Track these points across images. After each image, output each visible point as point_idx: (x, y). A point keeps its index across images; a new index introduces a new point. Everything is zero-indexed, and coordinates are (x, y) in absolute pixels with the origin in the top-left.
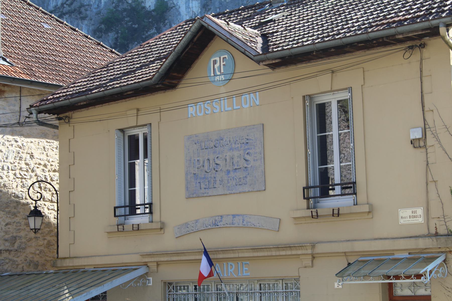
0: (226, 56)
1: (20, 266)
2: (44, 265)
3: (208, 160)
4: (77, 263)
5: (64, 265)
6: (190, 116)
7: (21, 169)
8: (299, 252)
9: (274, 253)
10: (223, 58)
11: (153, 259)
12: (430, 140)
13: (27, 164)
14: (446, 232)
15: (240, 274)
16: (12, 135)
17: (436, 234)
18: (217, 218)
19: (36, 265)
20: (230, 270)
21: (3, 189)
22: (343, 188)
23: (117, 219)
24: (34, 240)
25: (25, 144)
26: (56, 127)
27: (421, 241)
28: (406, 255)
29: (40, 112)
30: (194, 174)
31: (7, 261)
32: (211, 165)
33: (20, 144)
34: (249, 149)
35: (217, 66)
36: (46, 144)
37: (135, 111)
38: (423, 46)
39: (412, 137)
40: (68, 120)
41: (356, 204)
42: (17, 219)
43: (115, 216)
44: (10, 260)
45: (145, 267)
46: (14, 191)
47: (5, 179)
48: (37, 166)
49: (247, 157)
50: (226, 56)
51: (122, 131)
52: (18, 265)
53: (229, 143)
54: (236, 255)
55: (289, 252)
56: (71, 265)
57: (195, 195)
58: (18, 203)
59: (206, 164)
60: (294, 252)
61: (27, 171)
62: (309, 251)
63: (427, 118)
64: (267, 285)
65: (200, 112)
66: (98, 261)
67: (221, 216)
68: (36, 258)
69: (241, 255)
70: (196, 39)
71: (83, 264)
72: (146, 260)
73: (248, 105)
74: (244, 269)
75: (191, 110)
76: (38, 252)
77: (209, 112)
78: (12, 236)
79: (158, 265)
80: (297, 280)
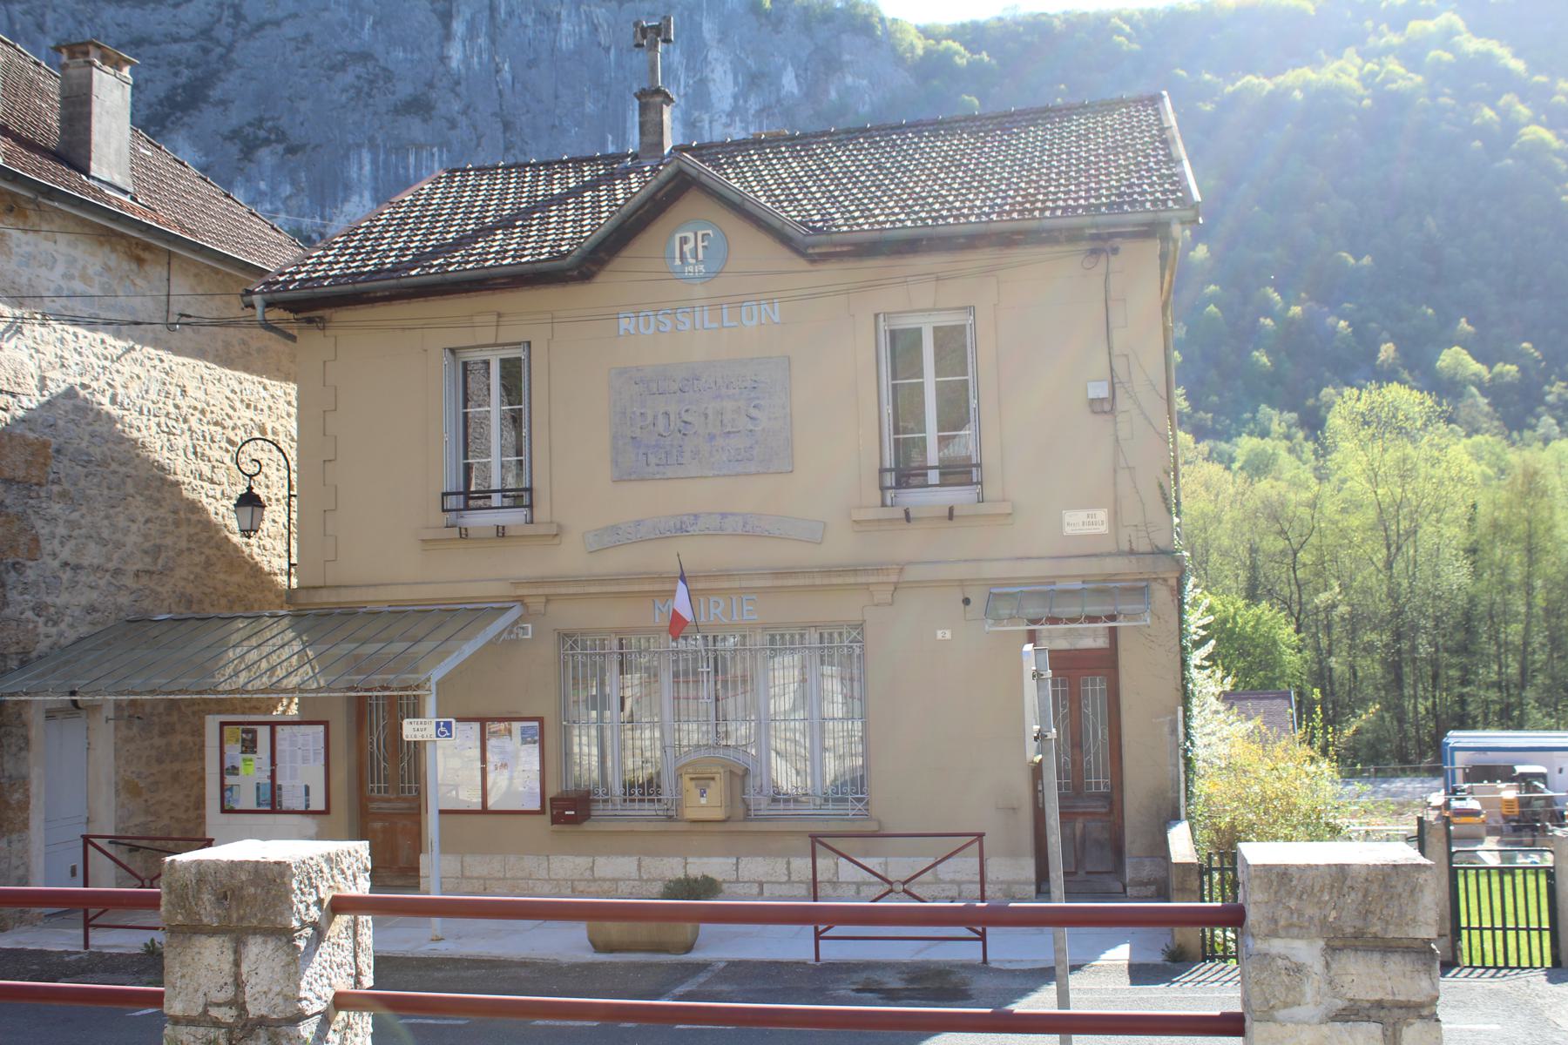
0: (710, 232)
1: (166, 603)
2: (200, 602)
3: (666, 414)
4: (346, 597)
5: (317, 600)
6: (622, 332)
7: (168, 414)
8: (873, 579)
9: (818, 581)
10: (703, 235)
11: (540, 591)
12: (1123, 403)
13: (177, 407)
14: (1148, 548)
15: (735, 618)
16: (155, 348)
17: (1132, 552)
18: (685, 518)
19: (190, 602)
20: (712, 610)
21: (139, 451)
22: (941, 474)
23: (448, 515)
24: (186, 553)
25: (174, 368)
26: (293, 338)
27: (1108, 560)
28: (1078, 585)
29: (269, 305)
30: (633, 438)
31: (147, 592)
32: (672, 424)
33: (166, 365)
34: (758, 398)
35: (687, 248)
36: (204, 370)
37: (494, 318)
38: (1115, 251)
39: (1091, 396)
40: (321, 324)
41: (981, 500)
42: (162, 512)
43: (443, 511)
44: (152, 591)
45: (518, 604)
46: (157, 458)
47: (144, 432)
48: (191, 411)
49: (754, 413)
50: (710, 232)
51: (453, 351)
52: (163, 600)
53: (713, 385)
54: (736, 584)
55: (851, 580)
56: (333, 599)
57: (633, 477)
58: (163, 480)
59: (661, 421)
60: (861, 579)
61: (177, 420)
62: (893, 578)
63: (1115, 367)
64: (787, 637)
65: (648, 326)
66: (401, 594)
67: (696, 516)
68: (190, 589)
69: (745, 584)
70: (662, 193)
71: (364, 599)
72: (521, 592)
73: (755, 322)
74: (745, 608)
75: (624, 323)
76: (192, 577)
77: (668, 328)
78: (155, 545)
79: (548, 601)
80: (860, 627)
